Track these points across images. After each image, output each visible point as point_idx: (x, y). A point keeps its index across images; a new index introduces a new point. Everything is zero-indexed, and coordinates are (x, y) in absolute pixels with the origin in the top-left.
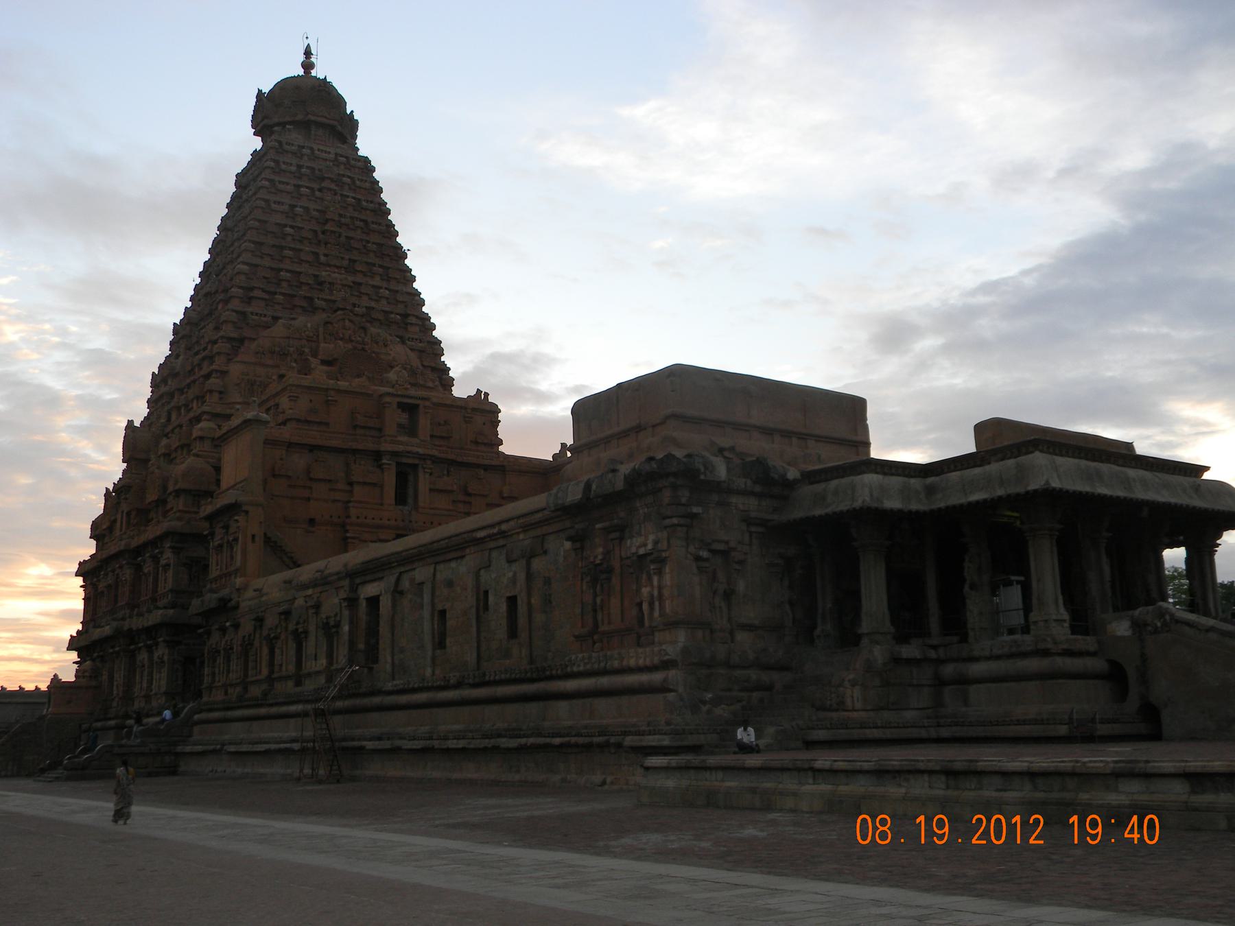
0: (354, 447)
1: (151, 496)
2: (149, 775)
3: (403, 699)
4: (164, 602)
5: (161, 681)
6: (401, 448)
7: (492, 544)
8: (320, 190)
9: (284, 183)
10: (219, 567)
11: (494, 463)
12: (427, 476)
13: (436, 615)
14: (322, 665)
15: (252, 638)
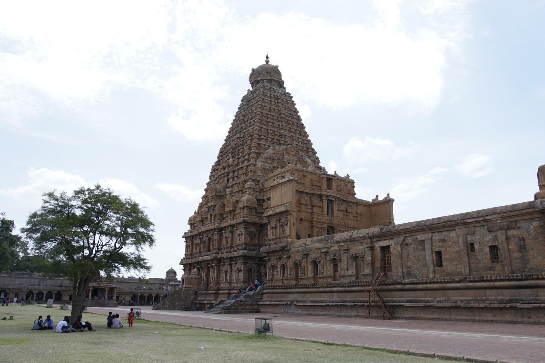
0: (313, 193)
1: (228, 209)
2: (250, 312)
3: (421, 286)
4: (241, 247)
5: (241, 276)
6: (329, 194)
7: (476, 225)
8: (278, 103)
9: (266, 100)
10: (275, 235)
11: (355, 201)
12: (336, 205)
13: (434, 253)
14: (353, 272)
15: (301, 261)
